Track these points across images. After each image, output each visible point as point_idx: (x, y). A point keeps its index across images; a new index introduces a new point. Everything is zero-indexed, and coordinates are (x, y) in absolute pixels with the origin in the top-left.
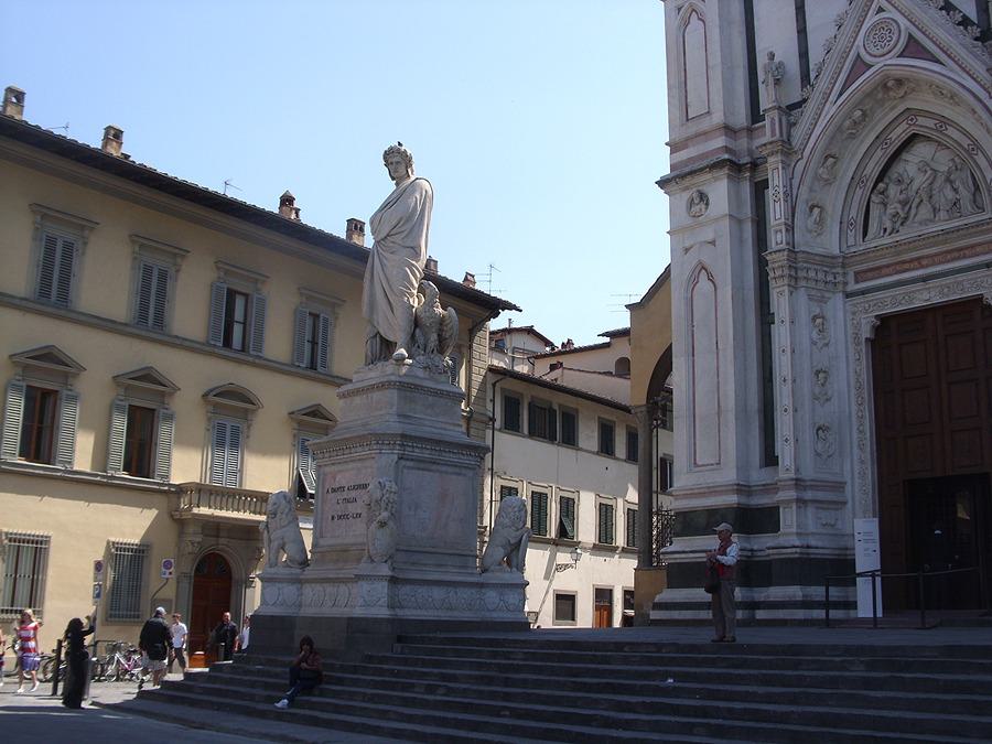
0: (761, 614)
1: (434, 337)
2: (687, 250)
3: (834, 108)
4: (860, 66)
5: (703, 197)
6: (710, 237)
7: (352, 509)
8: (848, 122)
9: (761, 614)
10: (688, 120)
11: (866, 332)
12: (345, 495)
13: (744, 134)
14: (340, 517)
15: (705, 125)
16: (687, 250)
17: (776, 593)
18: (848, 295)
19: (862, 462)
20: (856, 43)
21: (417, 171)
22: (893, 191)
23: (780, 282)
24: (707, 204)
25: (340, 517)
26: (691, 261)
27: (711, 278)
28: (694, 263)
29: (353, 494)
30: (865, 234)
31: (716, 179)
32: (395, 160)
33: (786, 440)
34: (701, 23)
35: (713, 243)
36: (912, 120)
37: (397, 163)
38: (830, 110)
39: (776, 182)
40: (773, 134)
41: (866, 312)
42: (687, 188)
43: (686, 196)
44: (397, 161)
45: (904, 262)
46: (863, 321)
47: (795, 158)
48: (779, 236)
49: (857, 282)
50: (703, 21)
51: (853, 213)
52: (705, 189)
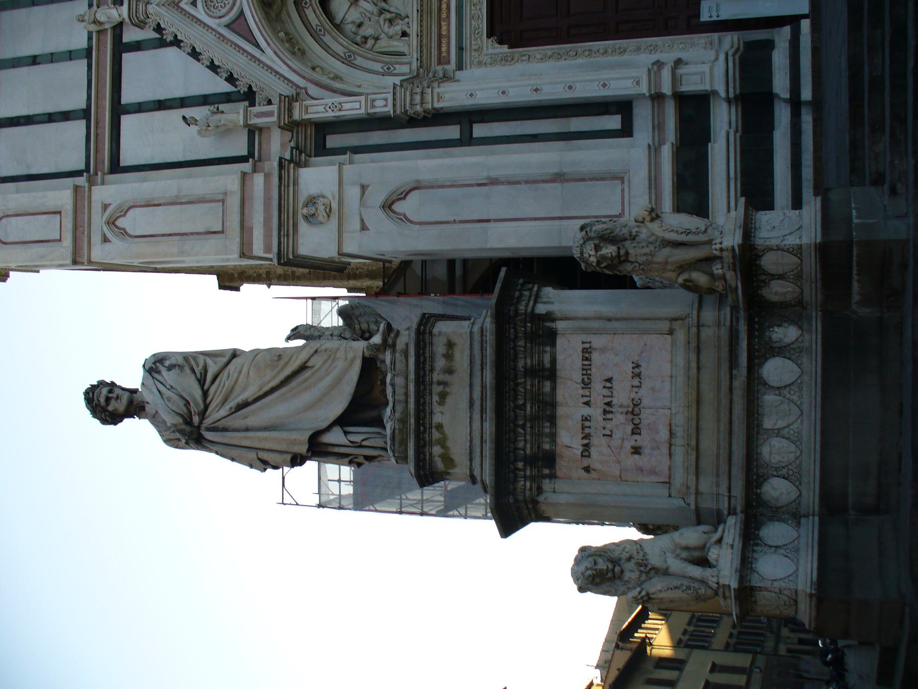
0: (806, 94)
2: (364, 228)
3: (269, 51)
4: (238, 25)
5: (312, 201)
6: (357, 191)
7: (622, 396)
8: (287, 45)
9: (806, 94)
10: (222, 232)
11: (505, 49)
12: (596, 412)
13: (258, 164)
14: (636, 431)
15: (234, 202)
16: (364, 228)
17: (781, 84)
18: (460, 67)
19: (638, 49)
20: (214, 26)
21: (131, 377)
22: (367, 31)
23: (428, 98)
24: (324, 197)
25: (636, 431)
26: (376, 217)
27: (403, 196)
28: (381, 214)
29: (597, 386)
30: (402, 54)
31: (296, 183)
32: (105, 391)
33: (604, 85)
34: (131, 213)
35: (364, 188)
36: (306, 3)
37: (110, 391)
38: (269, 56)
39: (321, 109)
40: (270, 114)
41: (479, 49)
42: (295, 226)
43: (303, 226)
44: (108, 404)
45: (440, 9)
46: (490, 51)
47: (303, 95)
48: (383, 103)
49: (448, 63)
50: (130, 208)
51: (377, 67)
52: (302, 199)
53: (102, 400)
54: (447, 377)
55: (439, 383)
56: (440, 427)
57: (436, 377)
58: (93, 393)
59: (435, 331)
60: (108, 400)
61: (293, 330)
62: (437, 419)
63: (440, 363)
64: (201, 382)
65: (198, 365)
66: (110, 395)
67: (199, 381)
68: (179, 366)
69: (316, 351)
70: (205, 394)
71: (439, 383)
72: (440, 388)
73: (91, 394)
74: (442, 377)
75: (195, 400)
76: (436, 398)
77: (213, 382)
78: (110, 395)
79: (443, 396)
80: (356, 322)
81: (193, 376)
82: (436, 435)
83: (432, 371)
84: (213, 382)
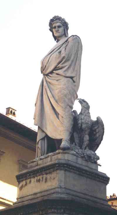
1: (87, 138)
21: (71, 32)
32: (58, 24)
37: (59, 27)
53: (53, 26)
54: (44, 180)
55: (43, 178)
56: (30, 182)
57: (45, 176)
58: (56, 20)
59: (58, 171)
60: (55, 27)
61: (83, 100)
62: (33, 180)
63: (48, 176)
64: (56, 69)
65: (63, 64)
66: (57, 27)
67: (56, 67)
68: (60, 56)
69: (63, 117)
70: (51, 72)
71: (43, 178)
72: (41, 179)
73: (55, 19)
74: (44, 178)
75: (47, 69)
76: (38, 178)
77: (57, 74)
78: (57, 27)
79: (39, 181)
80: (98, 126)
81: (56, 64)
82: (28, 181)
83: (46, 174)
84: (57, 74)
